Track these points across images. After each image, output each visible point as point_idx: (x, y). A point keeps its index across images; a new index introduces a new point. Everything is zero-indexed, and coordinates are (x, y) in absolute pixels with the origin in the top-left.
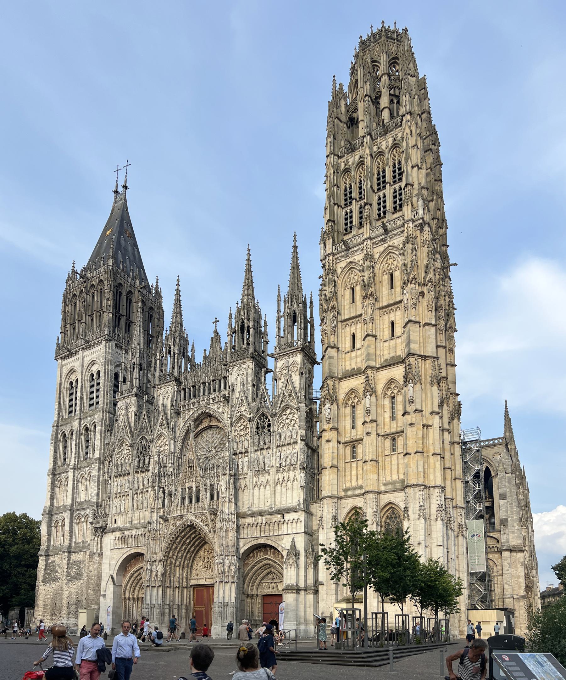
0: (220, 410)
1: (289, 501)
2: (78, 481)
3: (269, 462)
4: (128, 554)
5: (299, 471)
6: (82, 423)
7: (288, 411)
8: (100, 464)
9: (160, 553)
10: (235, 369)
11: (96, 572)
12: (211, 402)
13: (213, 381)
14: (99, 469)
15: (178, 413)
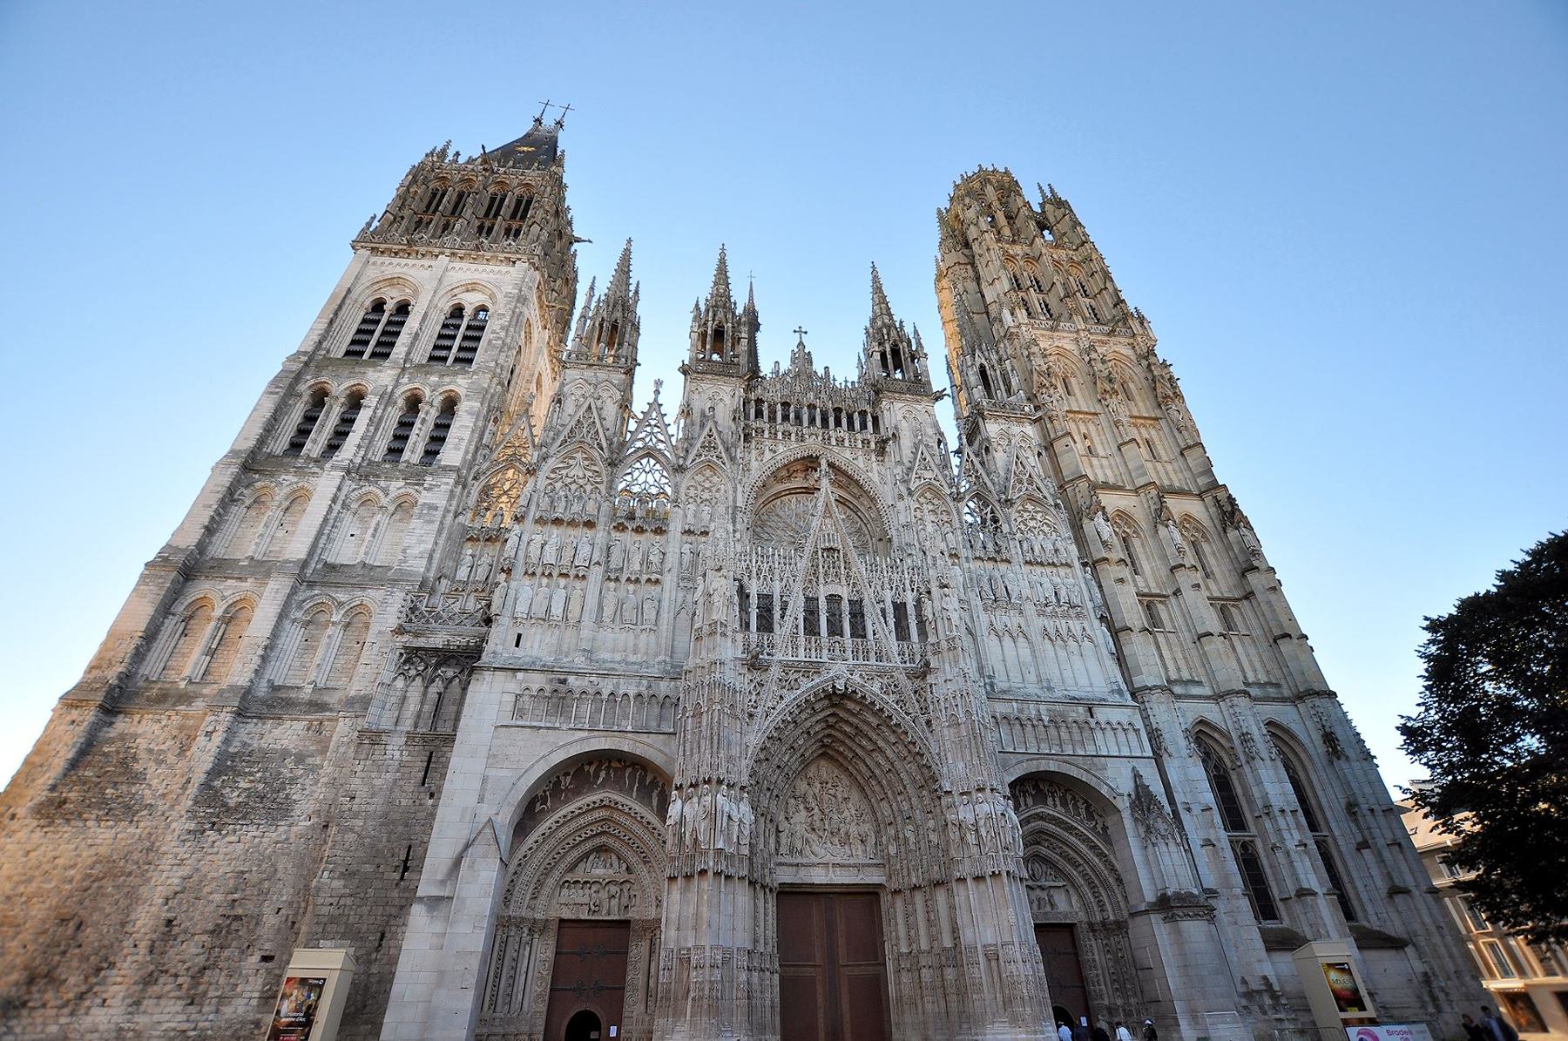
0: (862, 466)
1: (1083, 681)
2: (344, 505)
3: (1016, 588)
4: (574, 751)
5: (1097, 623)
6: (405, 380)
7: (1029, 507)
8: (457, 483)
9: (744, 762)
10: (898, 405)
11: (379, 800)
12: (834, 442)
13: (835, 410)
14: (452, 494)
15: (747, 437)
